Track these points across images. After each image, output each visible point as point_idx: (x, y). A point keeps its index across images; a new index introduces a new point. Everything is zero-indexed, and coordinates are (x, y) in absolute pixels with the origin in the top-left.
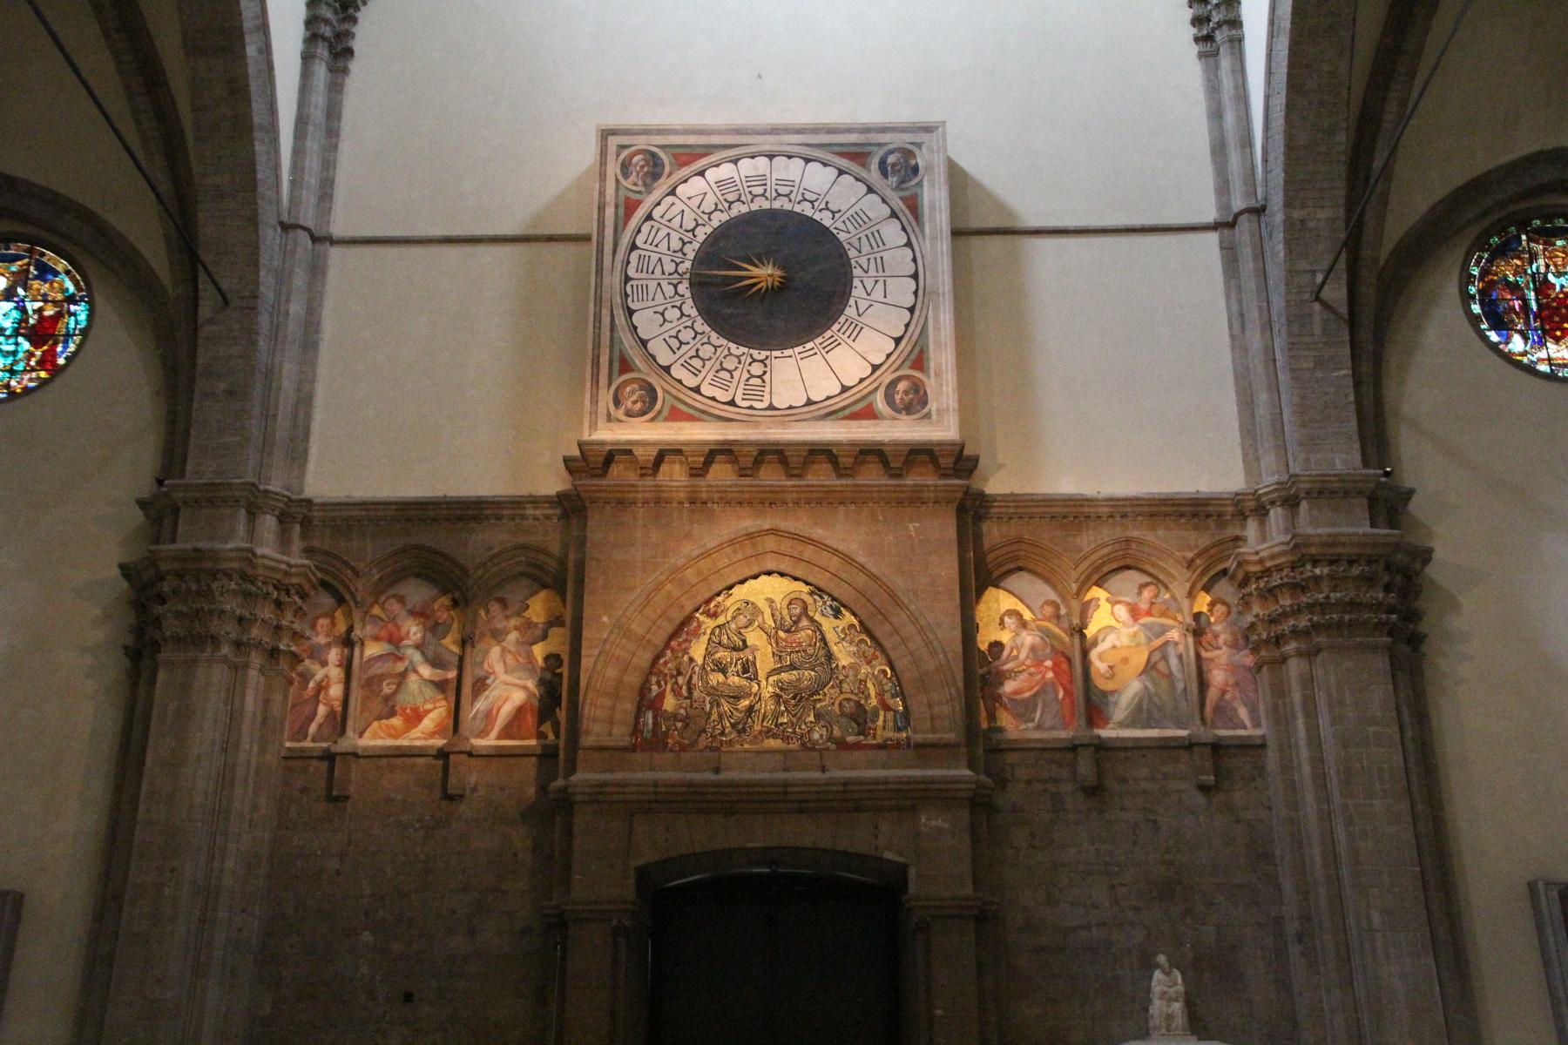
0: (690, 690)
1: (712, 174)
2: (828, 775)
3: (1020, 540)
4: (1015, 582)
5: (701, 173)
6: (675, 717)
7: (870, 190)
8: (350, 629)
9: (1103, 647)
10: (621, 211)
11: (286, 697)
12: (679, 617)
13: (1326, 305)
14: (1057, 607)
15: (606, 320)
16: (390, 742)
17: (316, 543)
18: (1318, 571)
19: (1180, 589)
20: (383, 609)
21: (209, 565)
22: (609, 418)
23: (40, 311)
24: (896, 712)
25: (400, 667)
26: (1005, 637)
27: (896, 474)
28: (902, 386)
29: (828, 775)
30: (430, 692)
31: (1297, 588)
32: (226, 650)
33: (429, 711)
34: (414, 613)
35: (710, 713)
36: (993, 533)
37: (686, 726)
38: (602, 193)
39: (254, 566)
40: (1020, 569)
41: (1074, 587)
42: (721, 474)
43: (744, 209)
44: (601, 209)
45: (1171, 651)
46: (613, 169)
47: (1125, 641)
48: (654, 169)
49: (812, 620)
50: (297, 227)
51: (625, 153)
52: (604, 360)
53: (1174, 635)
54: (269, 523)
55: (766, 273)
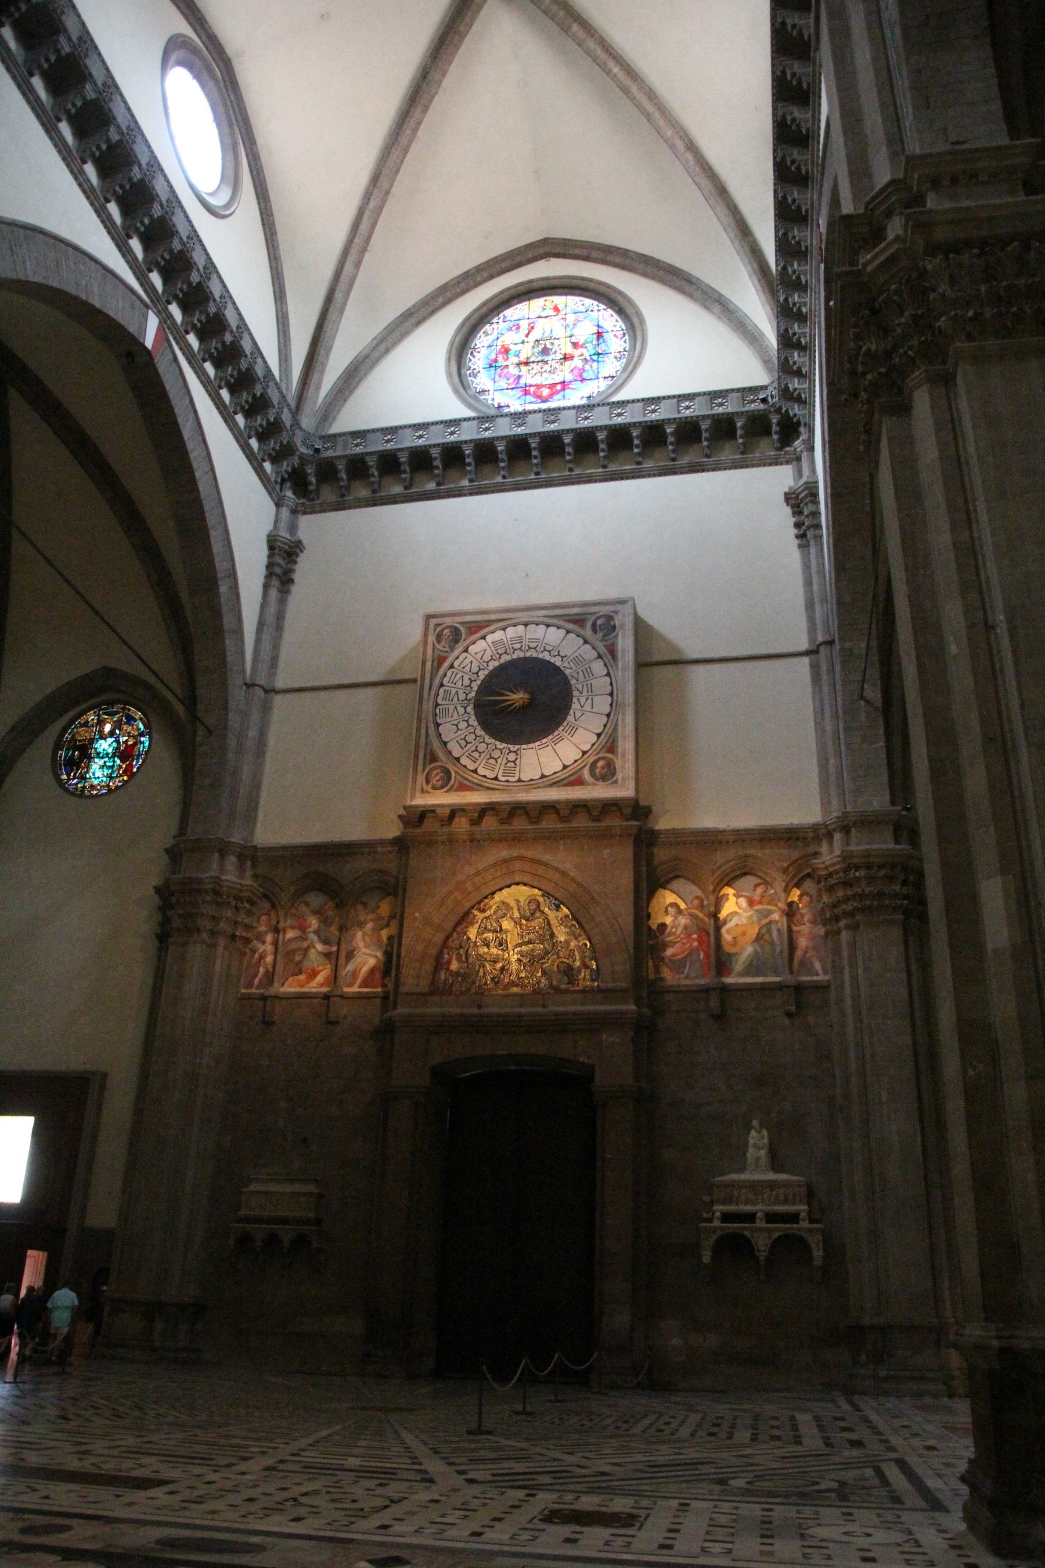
1: (489, 638)
2: (546, 1010)
3: (677, 858)
4: (676, 884)
5: (484, 638)
6: (457, 974)
7: (586, 642)
8: (278, 923)
10: (436, 663)
11: (241, 963)
12: (461, 911)
13: (867, 702)
14: (702, 901)
15: (423, 731)
16: (298, 989)
17: (259, 871)
18: (857, 874)
19: (779, 886)
20: (297, 910)
22: (423, 791)
23: (127, 741)
24: (592, 970)
25: (305, 945)
26: (668, 920)
27: (597, 819)
28: (600, 764)
29: (546, 1010)
30: (321, 959)
31: (847, 884)
32: (204, 936)
35: (478, 971)
36: (661, 854)
37: (464, 979)
38: (424, 654)
39: (221, 886)
40: (678, 877)
41: (711, 887)
42: (490, 823)
43: (508, 658)
45: (773, 926)
46: (432, 638)
47: (744, 921)
48: (456, 636)
49: (543, 912)
50: (254, 685)
53: (776, 916)
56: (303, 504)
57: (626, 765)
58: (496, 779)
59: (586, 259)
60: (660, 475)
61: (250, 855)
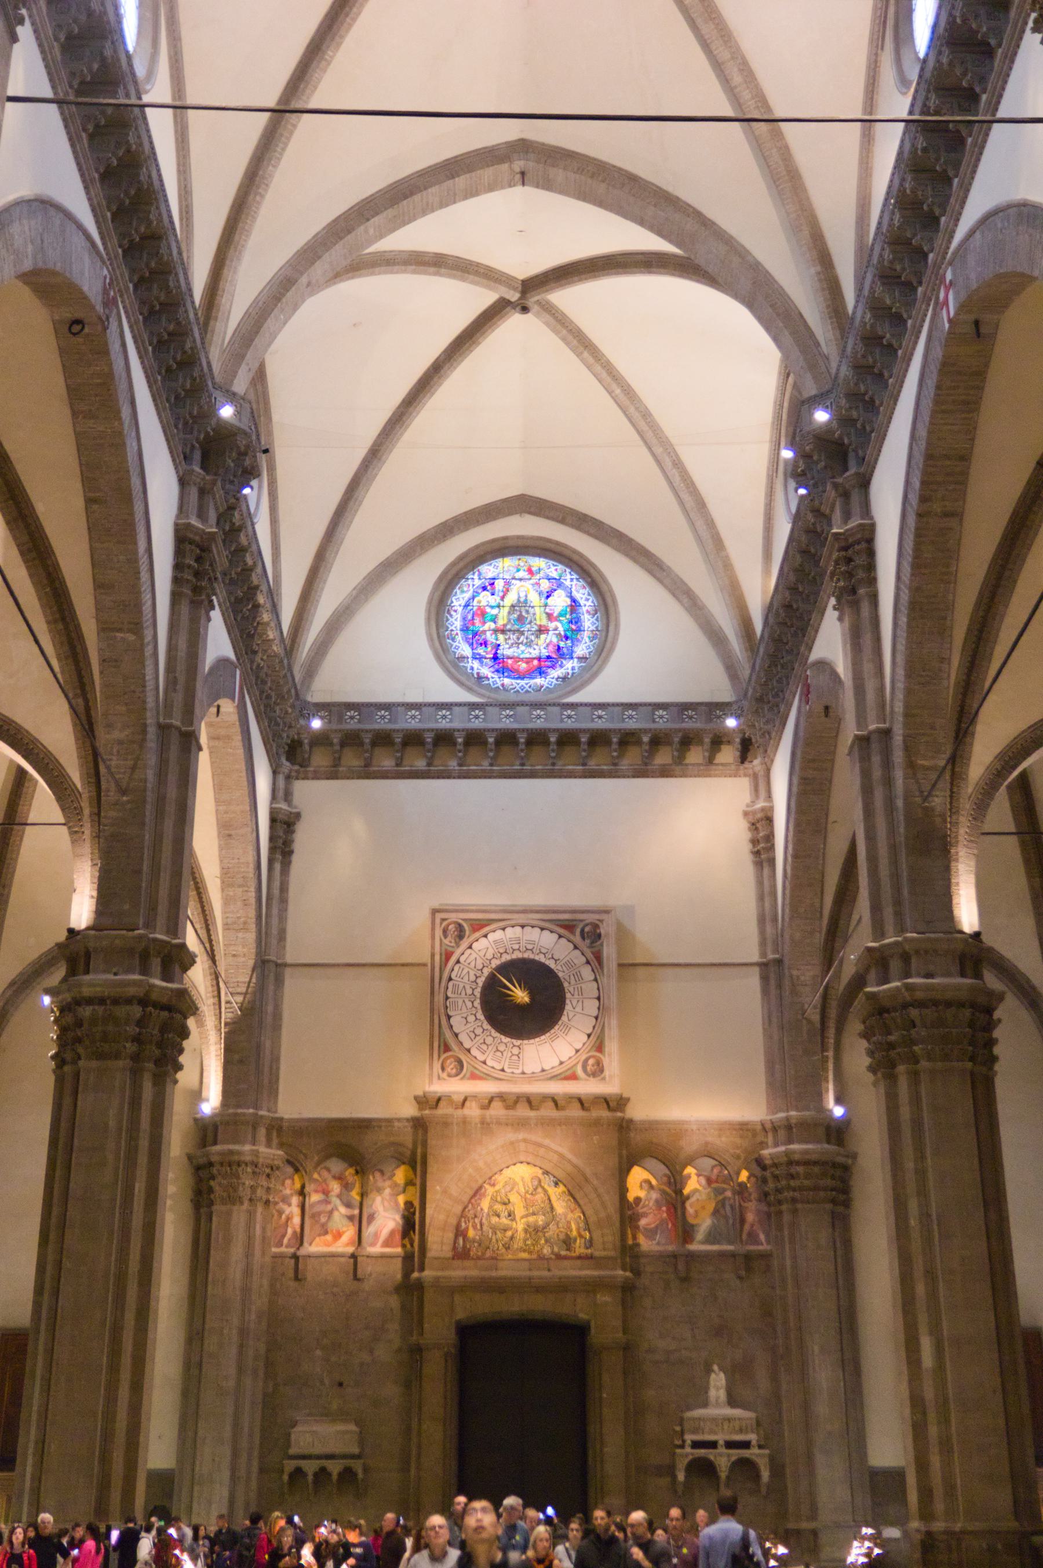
0: (481, 1225)
1: (491, 936)
6: (474, 1241)
7: (576, 947)
9: (693, 1200)
10: (444, 957)
12: (475, 1186)
15: (436, 1021)
21: (236, 1158)
25: (329, 1207)
26: (642, 1194)
28: (591, 1062)
30: (345, 1221)
33: (344, 1232)
34: (334, 1177)
37: (480, 1245)
38: (433, 947)
44: (433, 955)
45: (727, 1203)
46: (439, 933)
48: (461, 935)
51: (445, 923)
52: (436, 1044)
54: (262, 1132)
55: (521, 995)
58: (503, 1070)
61: (277, 1128)
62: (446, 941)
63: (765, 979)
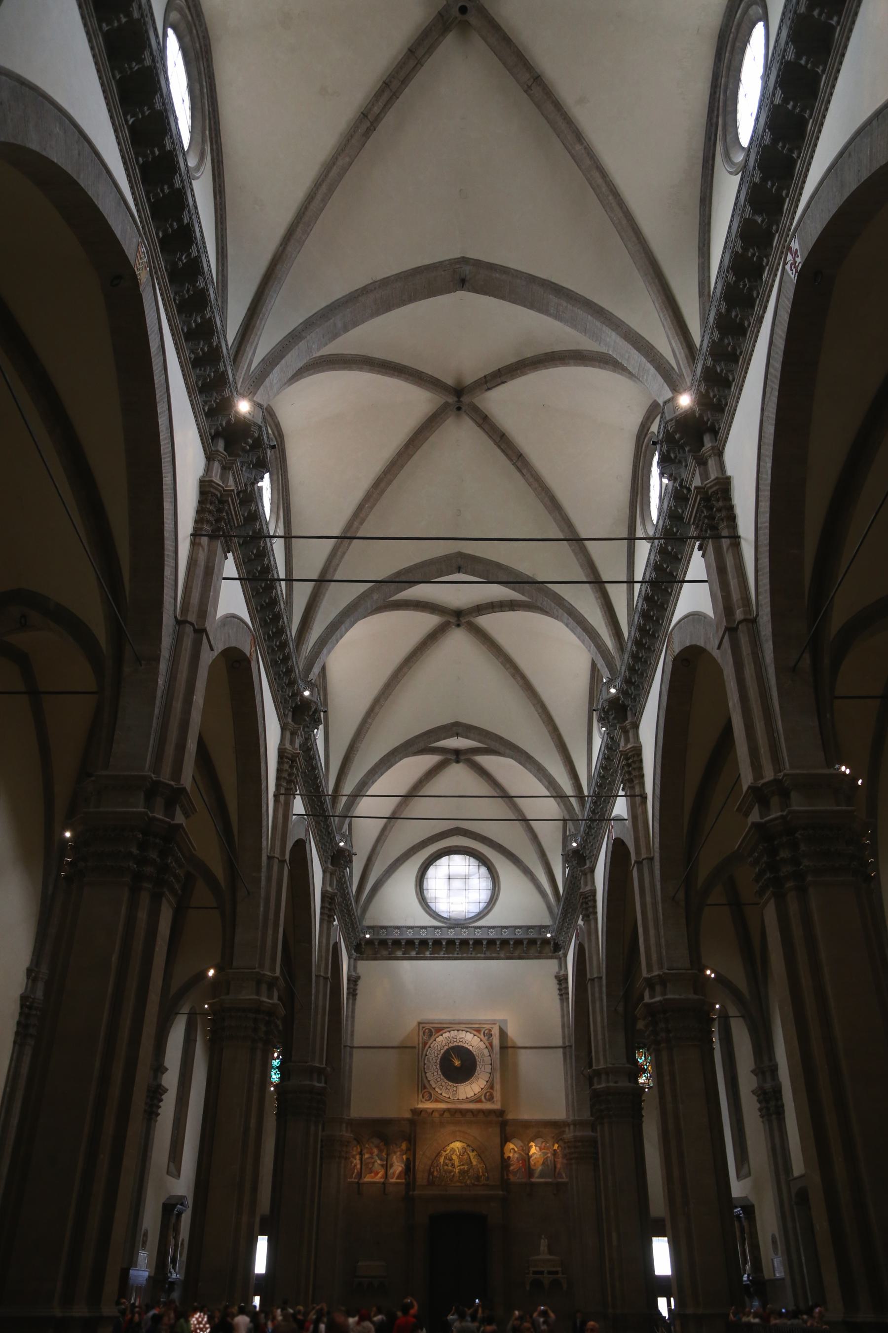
1: (444, 1035)
5: (442, 1035)
6: (437, 1177)
7: (481, 1041)
15: (420, 1077)
22: (422, 1101)
25: (373, 1160)
26: (511, 1155)
28: (488, 1094)
30: (380, 1167)
38: (419, 1040)
45: (549, 1159)
46: (421, 1033)
47: (538, 1156)
48: (431, 1035)
53: (549, 1155)
56: (359, 957)
57: (497, 1095)
58: (449, 1098)
59: (475, 839)
60: (507, 959)
61: (352, 1123)
62: (424, 1037)
63: (564, 1054)
